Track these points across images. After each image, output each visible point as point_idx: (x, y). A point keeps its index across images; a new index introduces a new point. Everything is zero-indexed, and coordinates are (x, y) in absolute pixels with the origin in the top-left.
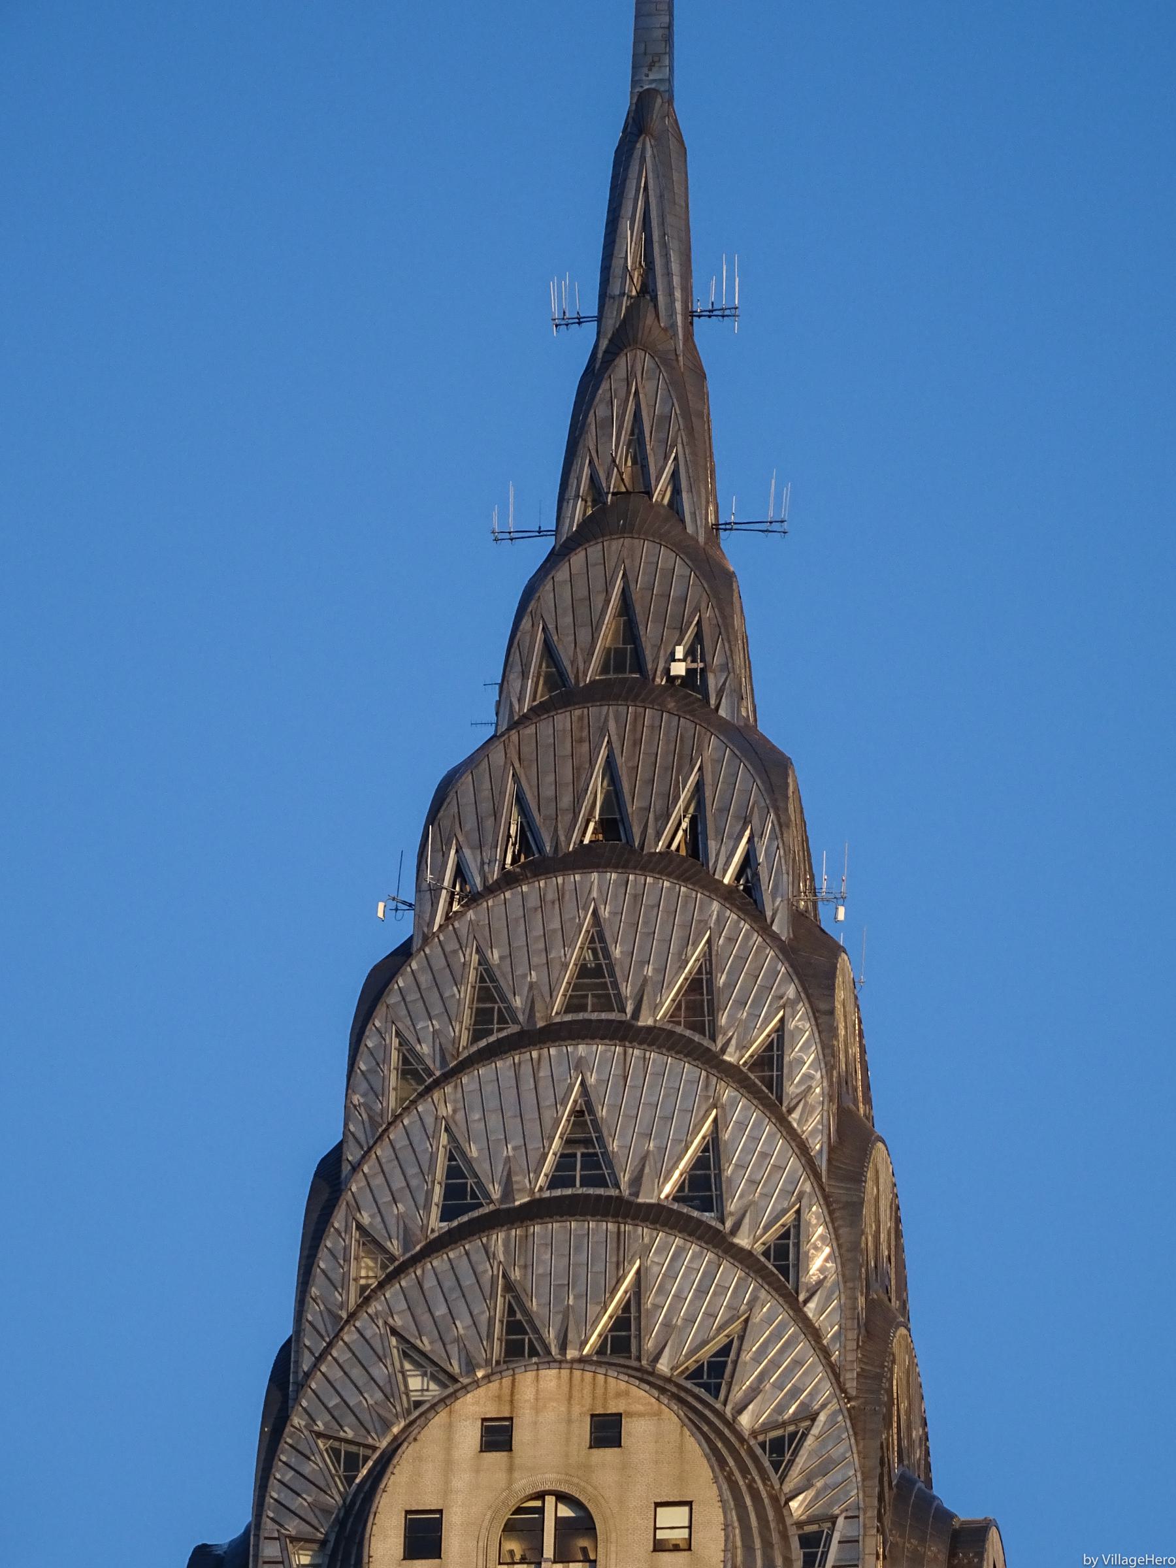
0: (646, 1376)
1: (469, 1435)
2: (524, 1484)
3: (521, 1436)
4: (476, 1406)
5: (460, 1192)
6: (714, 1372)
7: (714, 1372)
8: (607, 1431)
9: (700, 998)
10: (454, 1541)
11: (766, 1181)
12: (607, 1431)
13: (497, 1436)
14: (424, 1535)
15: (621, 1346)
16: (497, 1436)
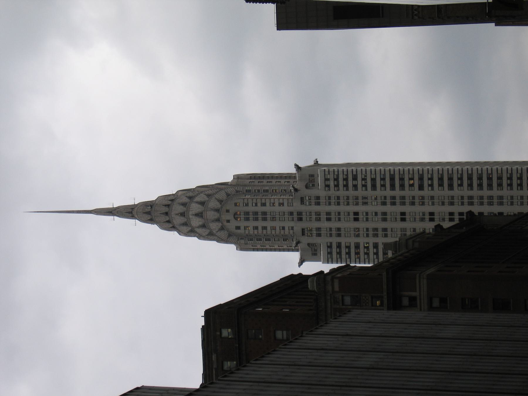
0: (222, 207)
1: (228, 224)
2: (233, 219)
3: (228, 219)
4: (225, 223)
5: (203, 226)
6: (221, 201)
7: (221, 201)
8: (228, 211)
9: (184, 204)
10: (238, 225)
11: (202, 198)
12: (228, 211)
13: (228, 221)
14: (238, 228)
15: (217, 210)
16: (228, 221)
